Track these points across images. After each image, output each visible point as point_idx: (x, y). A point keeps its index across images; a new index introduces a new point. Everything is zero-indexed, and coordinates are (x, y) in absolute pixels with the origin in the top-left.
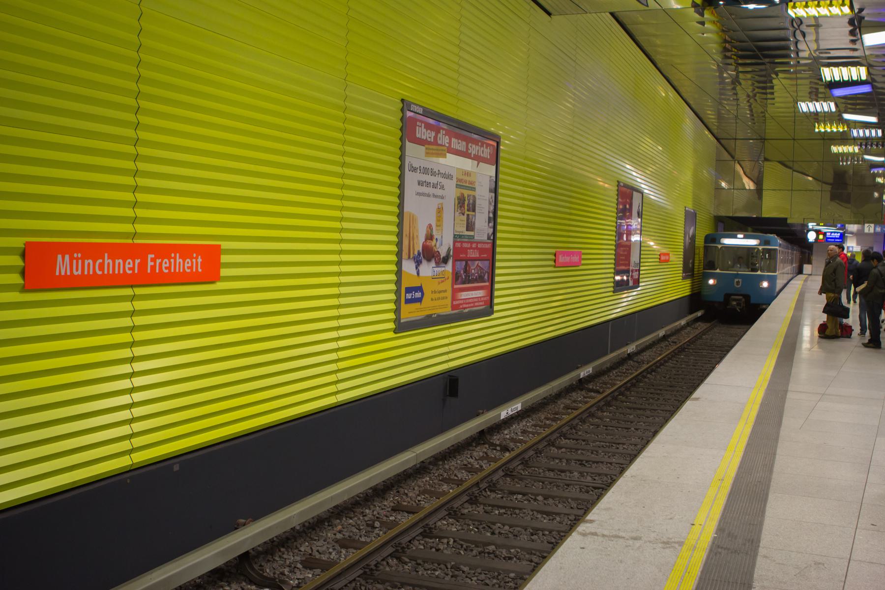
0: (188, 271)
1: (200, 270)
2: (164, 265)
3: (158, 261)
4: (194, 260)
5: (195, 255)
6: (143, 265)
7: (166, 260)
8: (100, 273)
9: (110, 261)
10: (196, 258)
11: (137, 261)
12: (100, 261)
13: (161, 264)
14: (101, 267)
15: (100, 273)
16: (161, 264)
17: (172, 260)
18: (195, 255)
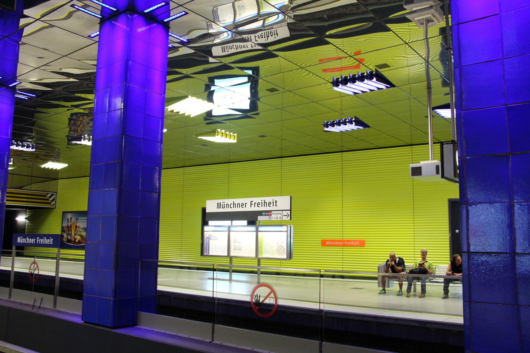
0: (33, 243)
1: (52, 243)
2: (41, 241)
3: (40, 240)
4: (50, 240)
5: (50, 238)
6: (36, 241)
7: (42, 239)
8: (26, 242)
9: (28, 239)
10: (51, 239)
11: (35, 239)
12: (26, 239)
13: (41, 241)
14: (27, 240)
15: (26, 242)
16: (41, 241)
17: (44, 240)
18: (50, 238)
